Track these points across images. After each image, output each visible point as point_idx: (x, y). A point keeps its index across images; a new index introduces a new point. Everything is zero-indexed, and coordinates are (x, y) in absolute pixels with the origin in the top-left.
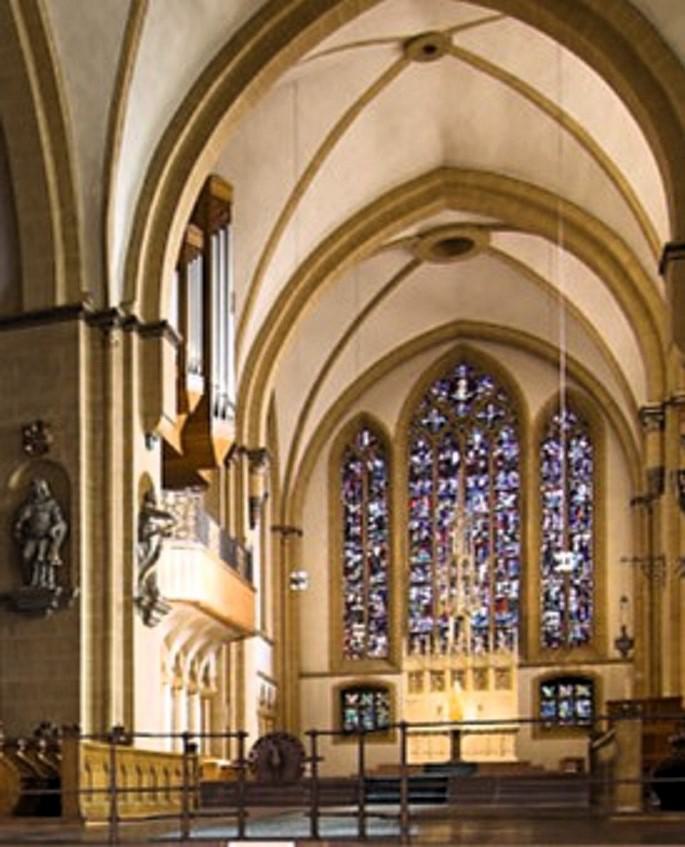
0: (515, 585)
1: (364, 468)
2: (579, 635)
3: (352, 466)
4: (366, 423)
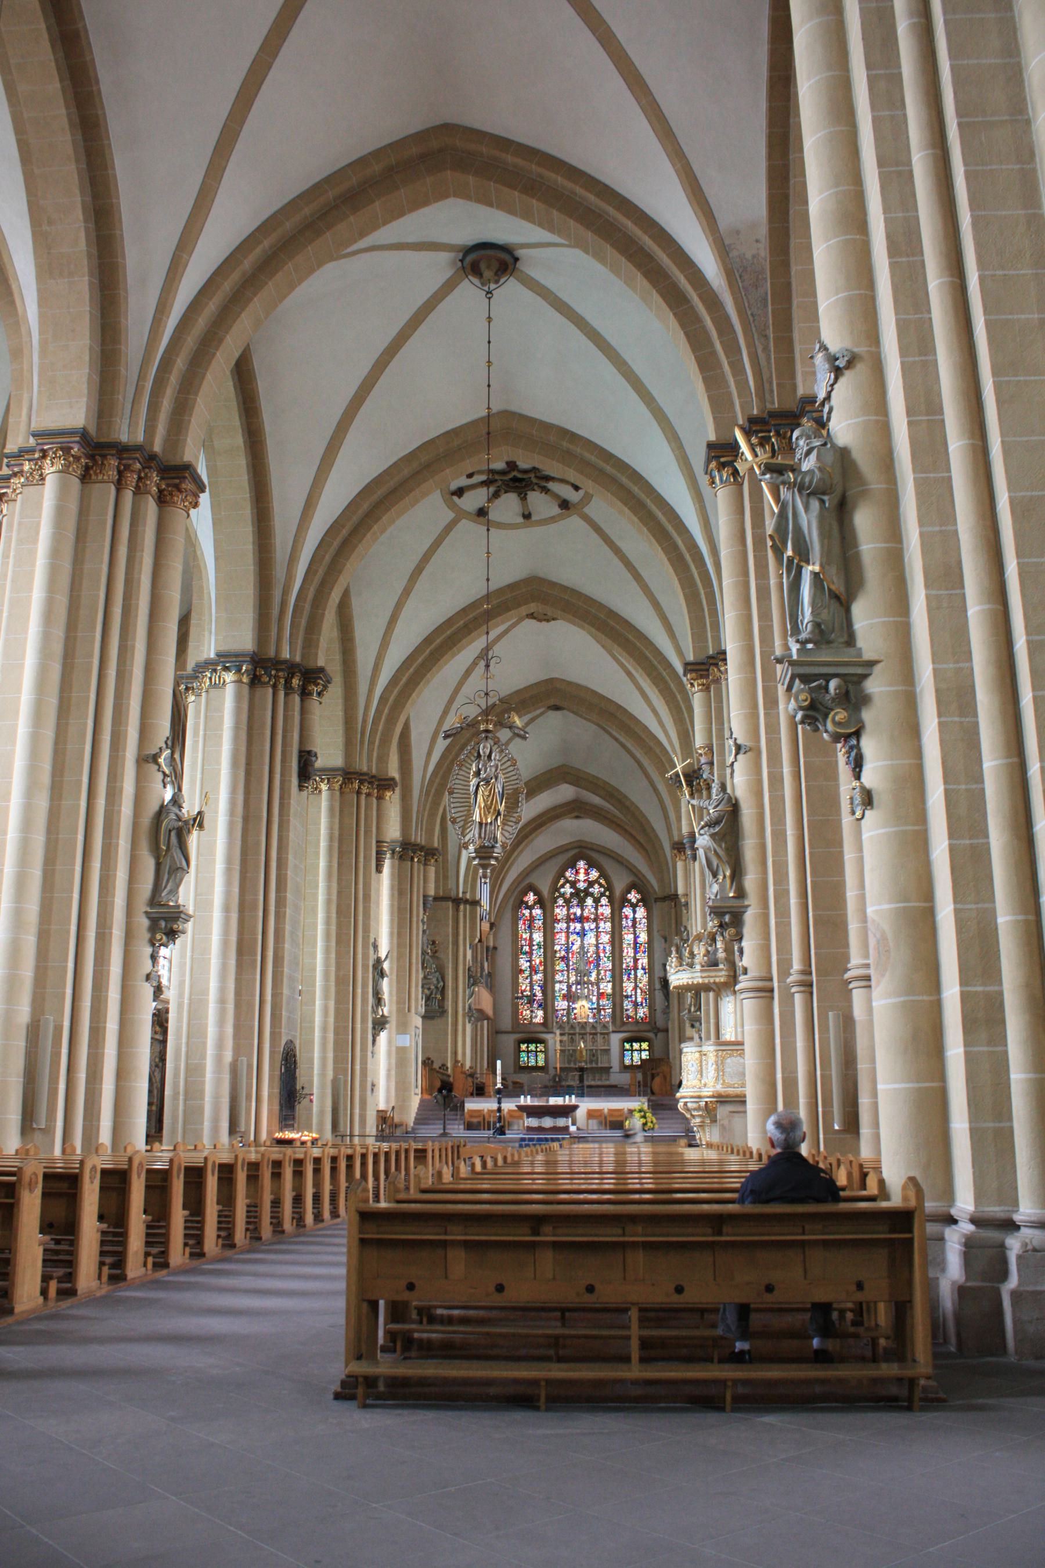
0: (610, 985)
1: (531, 913)
2: (642, 1015)
3: (524, 911)
4: (531, 888)
